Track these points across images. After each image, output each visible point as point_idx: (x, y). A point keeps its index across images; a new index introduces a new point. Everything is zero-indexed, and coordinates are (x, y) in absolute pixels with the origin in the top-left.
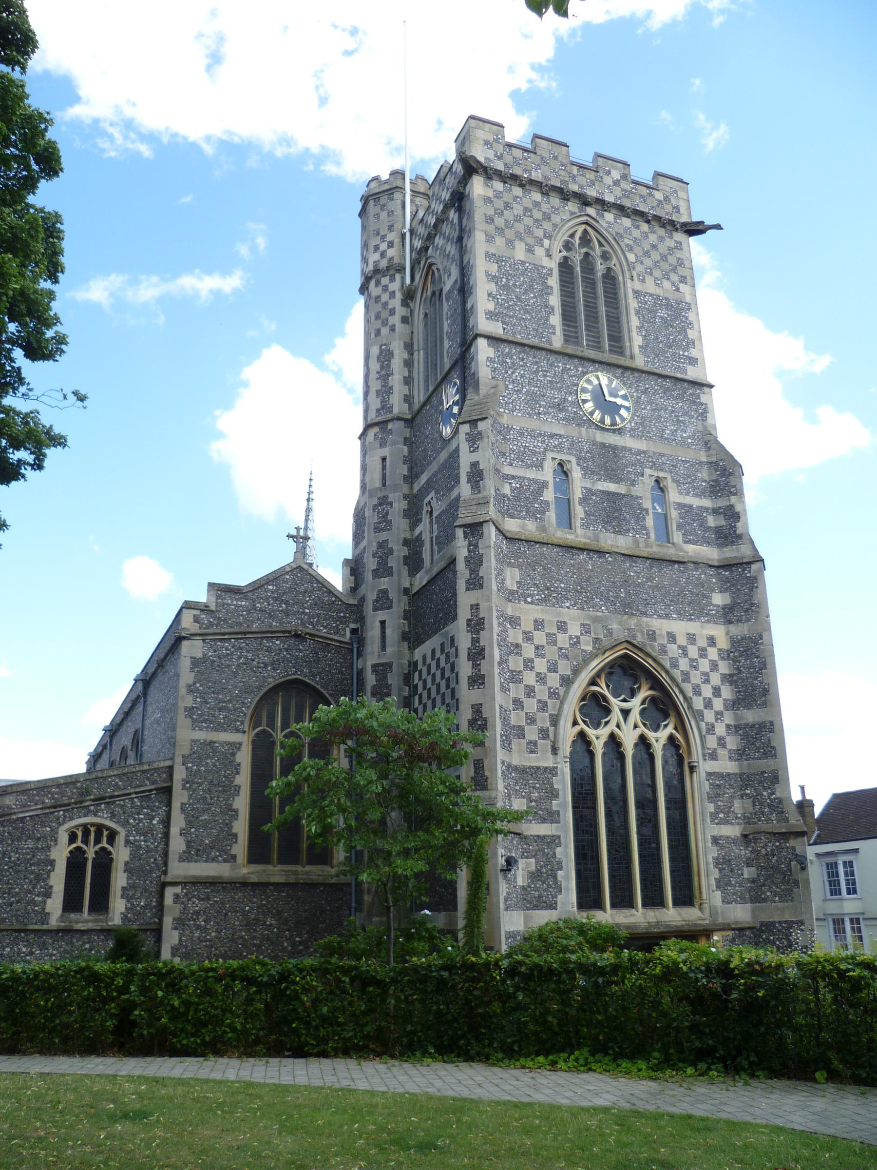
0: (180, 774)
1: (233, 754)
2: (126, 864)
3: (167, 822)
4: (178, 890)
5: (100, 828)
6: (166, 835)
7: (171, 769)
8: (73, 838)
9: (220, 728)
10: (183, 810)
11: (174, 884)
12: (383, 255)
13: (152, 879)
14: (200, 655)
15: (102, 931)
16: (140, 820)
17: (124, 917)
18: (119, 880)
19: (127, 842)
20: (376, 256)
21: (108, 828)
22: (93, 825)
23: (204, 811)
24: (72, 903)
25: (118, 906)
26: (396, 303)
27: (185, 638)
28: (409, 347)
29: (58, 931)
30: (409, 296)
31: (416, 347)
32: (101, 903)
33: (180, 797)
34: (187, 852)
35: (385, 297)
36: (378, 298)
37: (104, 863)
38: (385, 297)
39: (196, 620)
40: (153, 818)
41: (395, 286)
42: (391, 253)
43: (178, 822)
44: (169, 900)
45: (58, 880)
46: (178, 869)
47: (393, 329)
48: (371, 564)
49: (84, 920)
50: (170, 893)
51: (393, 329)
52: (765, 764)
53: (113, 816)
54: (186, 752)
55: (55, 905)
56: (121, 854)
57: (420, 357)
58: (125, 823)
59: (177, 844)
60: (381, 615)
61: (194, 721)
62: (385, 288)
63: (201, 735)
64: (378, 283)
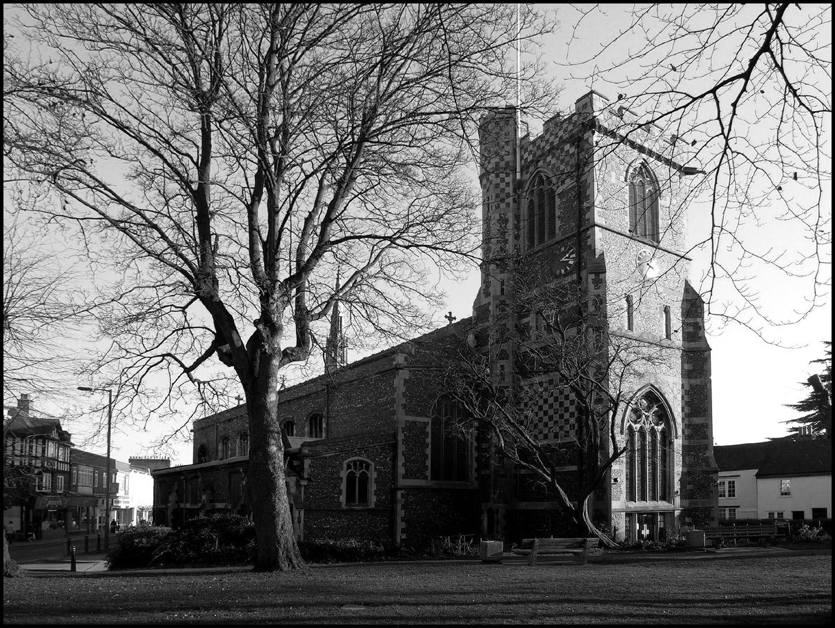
0: (401, 437)
1: (425, 428)
2: (376, 479)
3: (394, 459)
4: (403, 492)
5: (362, 462)
6: (394, 467)
7: (395, 436)
8: (349, 467)
9: (419, 415)
10: (403, 454)
11: (400, 489)
12: (502, 159)
13: (389, 487)
14: (408, 378)
15: (366, 510)
16: (381, 459)
17: (376, 504)
18: (373, 487)
19: (375, 469)
20: (497, 160)
21: (366, 462)
22: (358, 460)
23: (413, 455)
24: (350, 498)
25: (373, 499)
26: (510, 190)
27: (401, 369)
28: (517, 217)
29: (347, 510)
30: (519, 185)
31: (522, 218)
32: (364, 497)
33: (401, 448)
34: (406, 474)
35: (503, 185)
36: (497, 186)
37: (364, 480)
38: (503, 185)
39: (406, 360)
40: (386, 458)
41: (509, 179)
42: (507, 158)
43: (401, 460)
44: (399, 496)
45: (343, 486)
46: (402, 482)
47: (508, 205)
48: (493, 336)
49: (357, 507)
50: (399, 493)
51: (508, 205)
52: (704, 442)
53: (368, 457)
54: (404, 426)
55: (343, 498)
56: (373, 475)
57: (524, 224)
58: (373, 460)
59: (401, 471)
60: (502, 362)
61: (406, 411)
62: (503, 180)
63: (411, 418)
64: (497, 176)
